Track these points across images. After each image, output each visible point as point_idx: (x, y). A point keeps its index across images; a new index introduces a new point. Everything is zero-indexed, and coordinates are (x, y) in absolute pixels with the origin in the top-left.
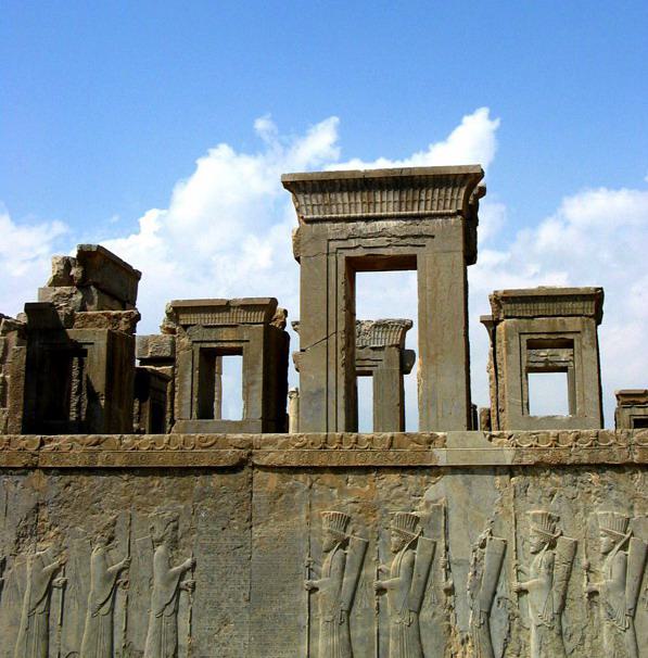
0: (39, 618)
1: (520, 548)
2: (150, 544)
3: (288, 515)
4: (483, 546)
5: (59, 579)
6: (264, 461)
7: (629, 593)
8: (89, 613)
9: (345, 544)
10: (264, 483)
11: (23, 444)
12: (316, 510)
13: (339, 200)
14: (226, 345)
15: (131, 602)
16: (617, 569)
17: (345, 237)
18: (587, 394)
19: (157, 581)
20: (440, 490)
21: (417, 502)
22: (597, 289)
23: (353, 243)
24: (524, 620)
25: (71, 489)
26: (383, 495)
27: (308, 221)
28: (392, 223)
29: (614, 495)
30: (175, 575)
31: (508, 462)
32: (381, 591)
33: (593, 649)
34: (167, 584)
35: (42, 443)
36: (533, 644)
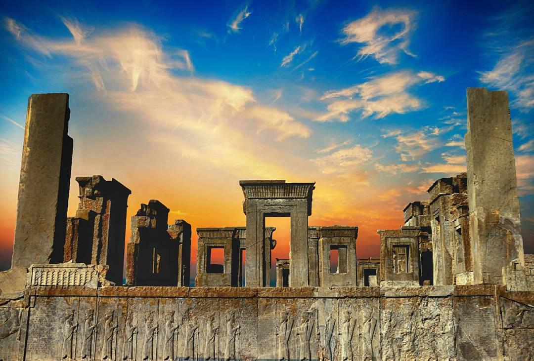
0: (190, 344)
1: (340, 322)
2: (226, 321)
3: (269, 312)
4: (328, 321)
5: (196, 332)
6: (262, 295)
7: (371, 335)
8: (207, 342)
9: (287, 321)
10: (261, 302)
11: (183, 290)
12: (278, 311)
13: (261, 191)
14: (218, 245)
15: (221, 339)
16: (368, 327)
17: (263, 205)
18: (352, 266)
19: (228, 332)
20: (316, 304)
21: (309, 308)
22: (356, 227)
23: (267, 207)
24: (340, 342)
25: (199, 304)
26: (298, 307)
27: (249, 199)
28: (281, 200)
29: (367, 306)
30: (234, 331)
31: (337, 296)
32: (298, 334)
33: (360, 350)
34: (232, 334)
35: (190, 289)
36: (343, 349)
